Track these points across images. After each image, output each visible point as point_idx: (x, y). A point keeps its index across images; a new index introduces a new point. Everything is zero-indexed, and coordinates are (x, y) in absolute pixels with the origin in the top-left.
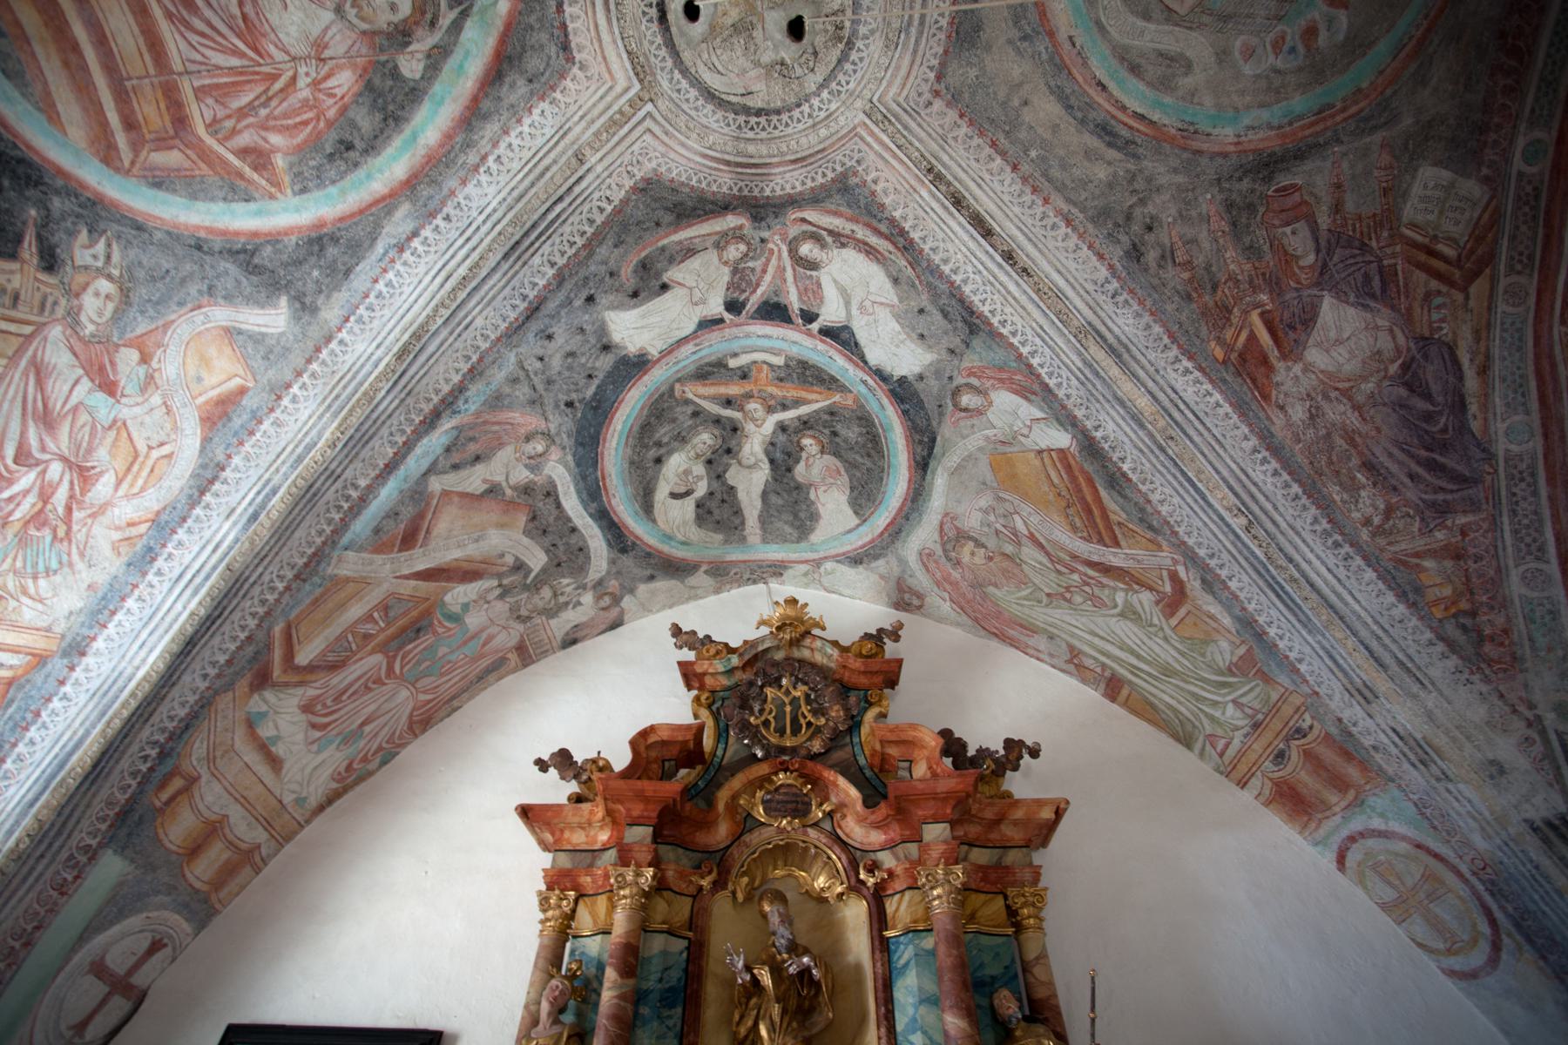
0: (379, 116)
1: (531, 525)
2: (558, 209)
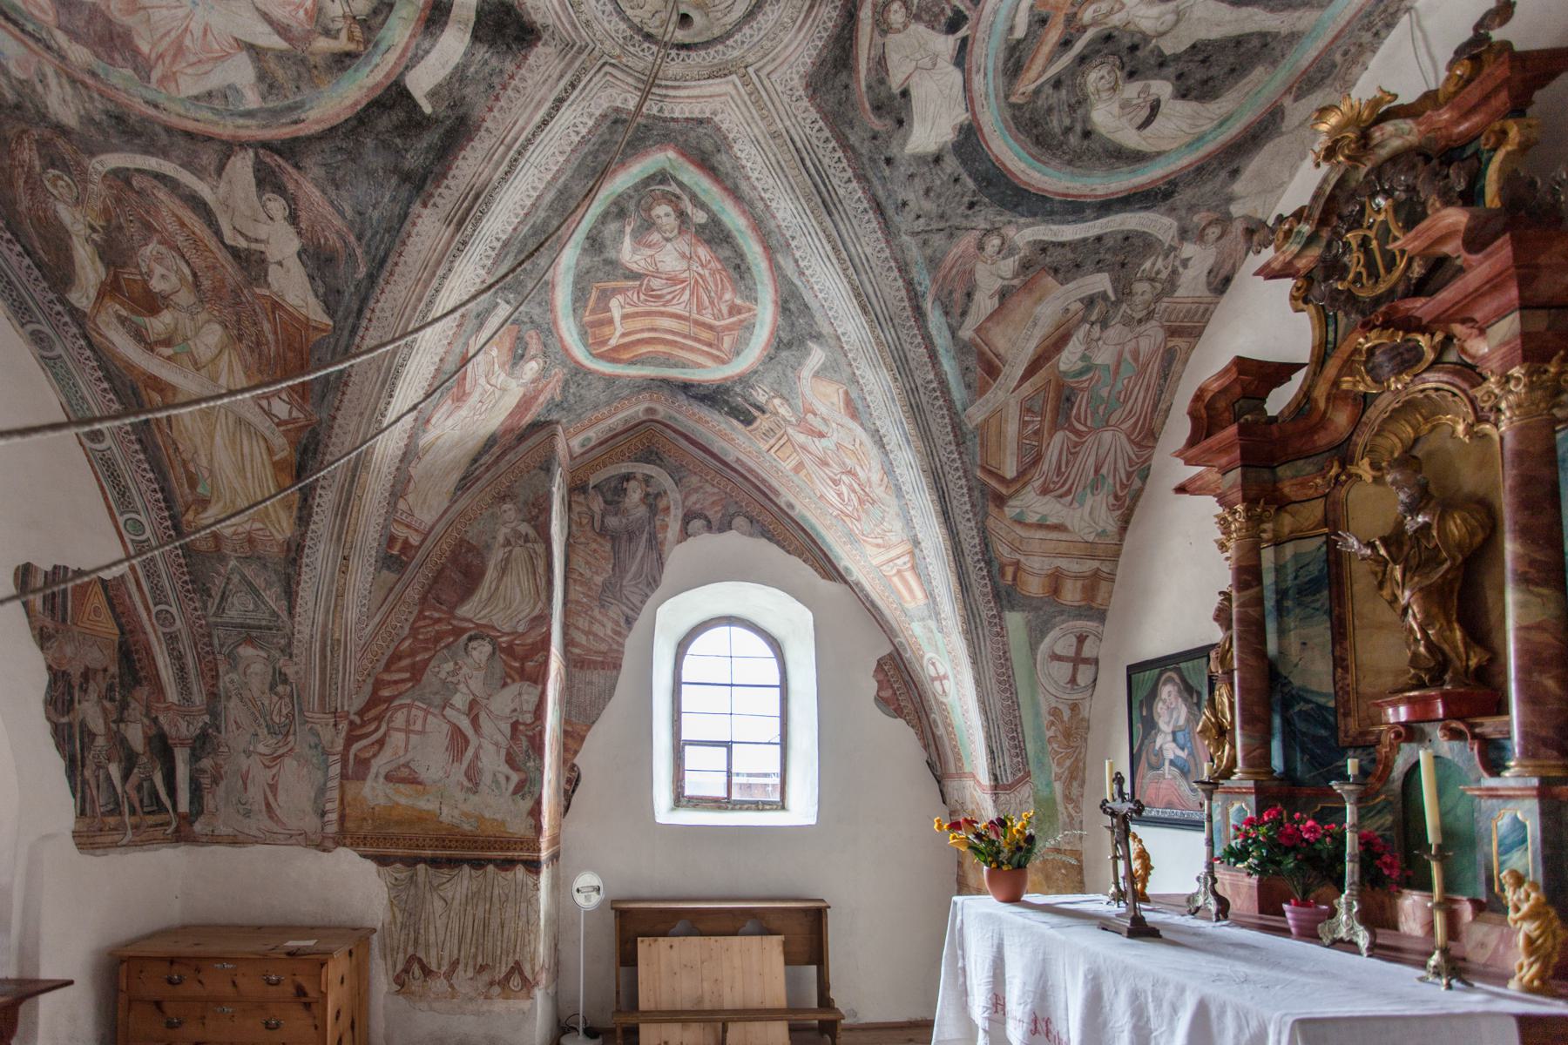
1: (1060, 276)
2: (809, 164)
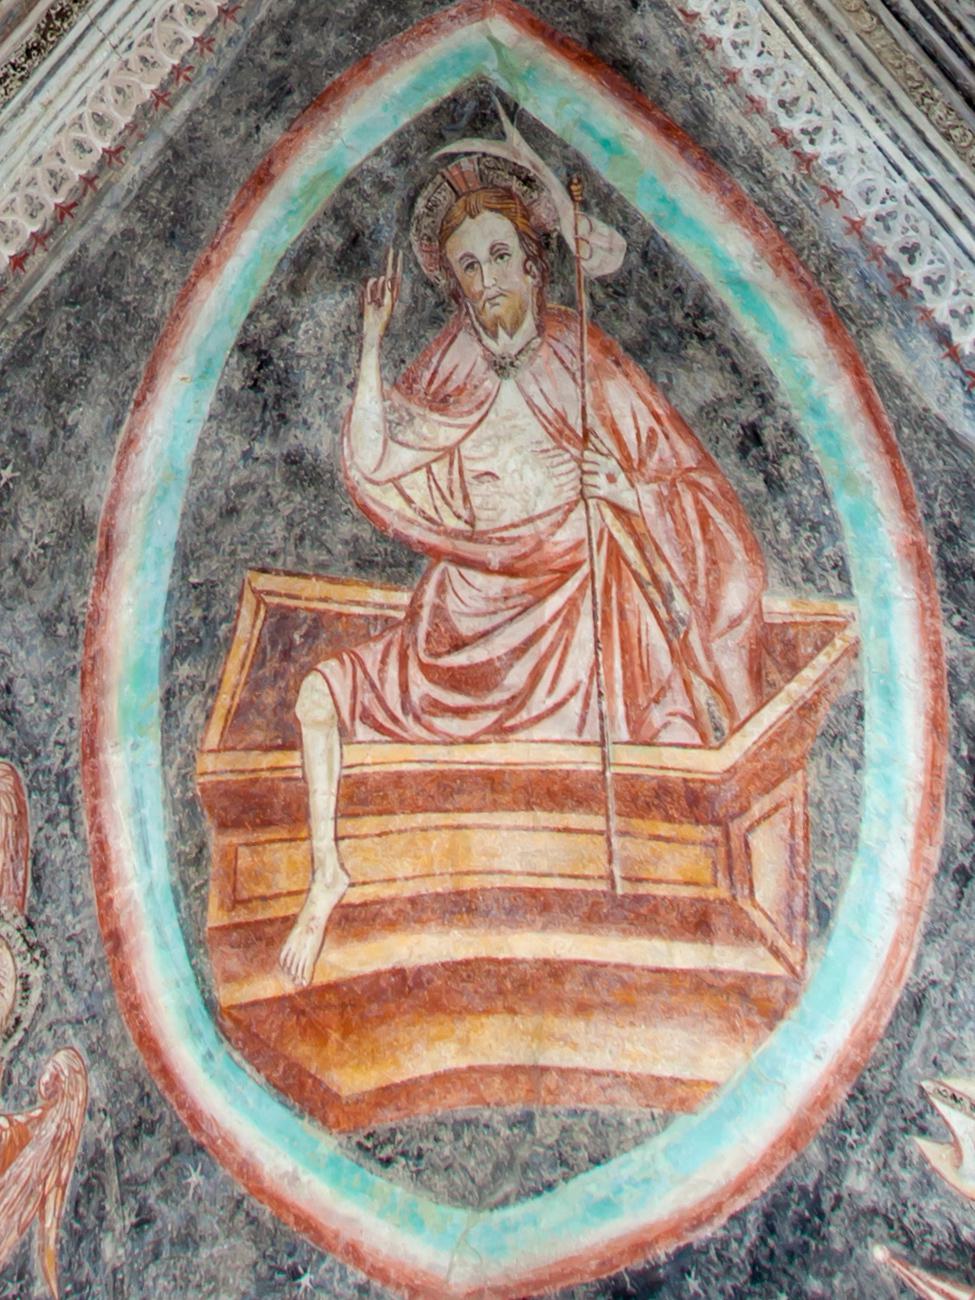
0: (694, 350)
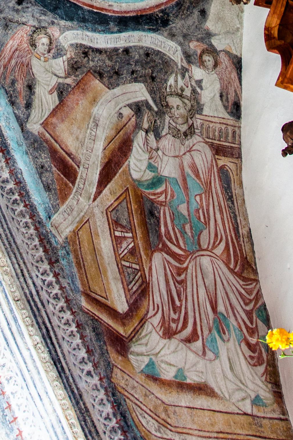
1: (105, 80)
